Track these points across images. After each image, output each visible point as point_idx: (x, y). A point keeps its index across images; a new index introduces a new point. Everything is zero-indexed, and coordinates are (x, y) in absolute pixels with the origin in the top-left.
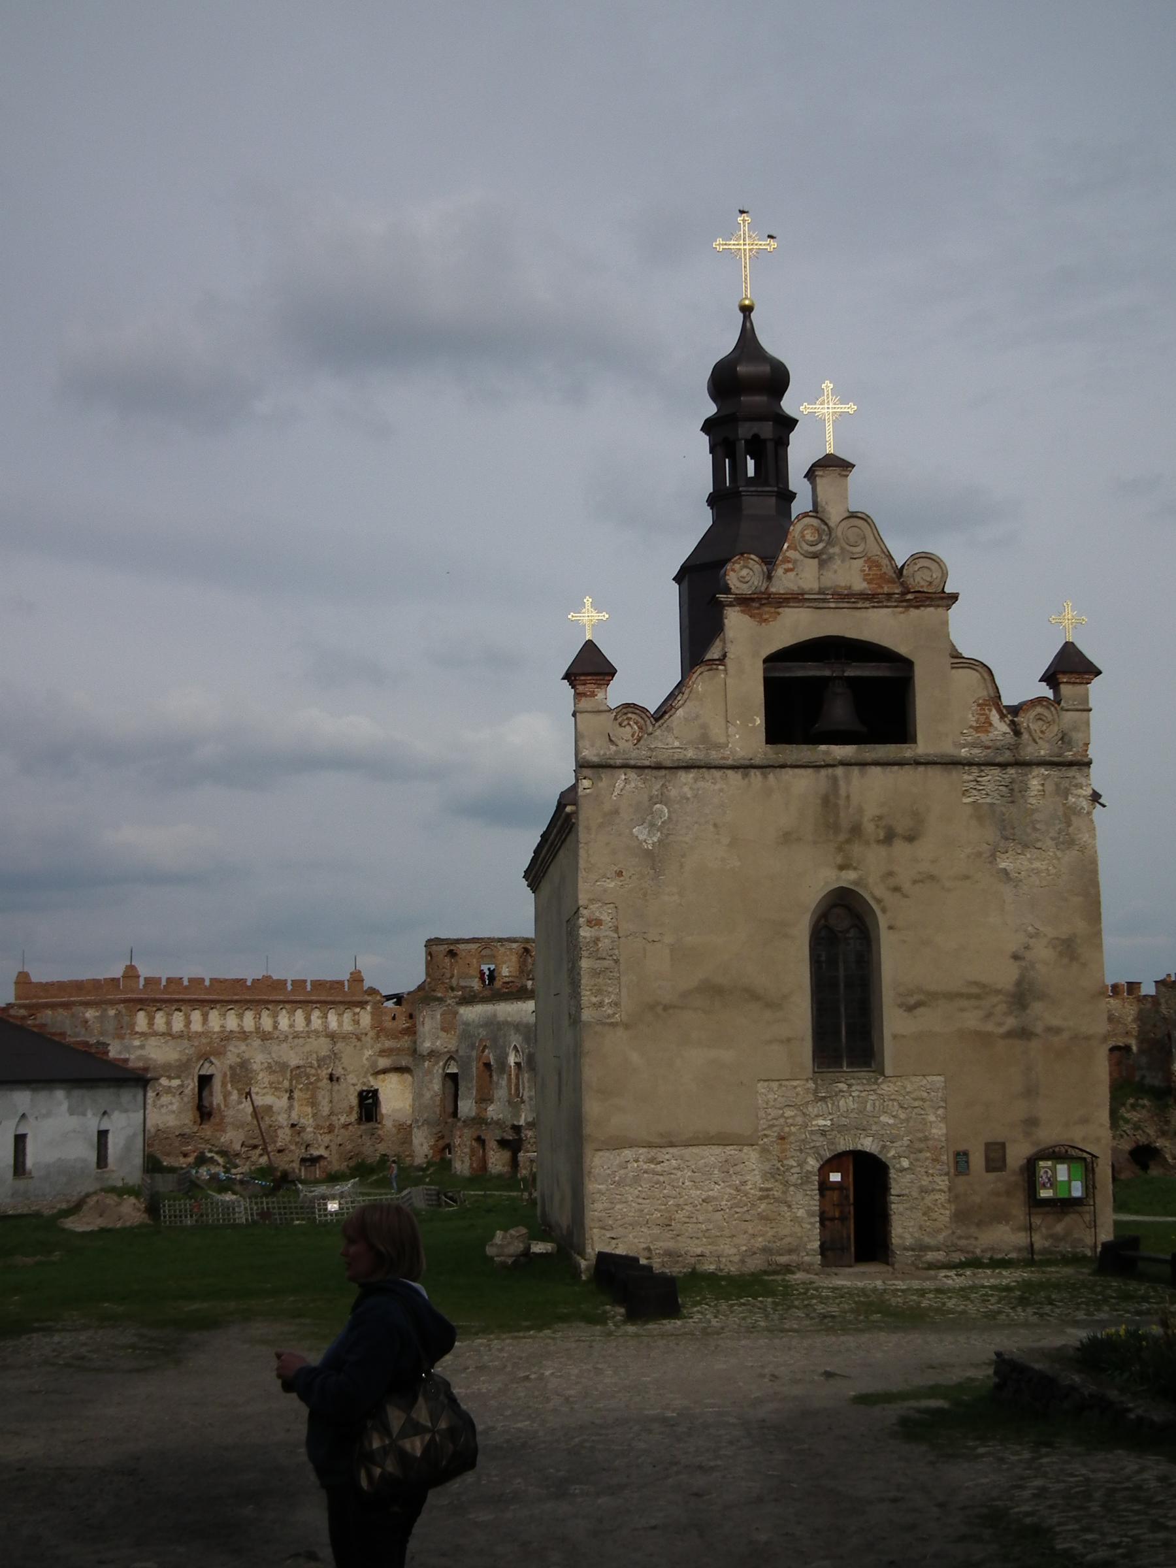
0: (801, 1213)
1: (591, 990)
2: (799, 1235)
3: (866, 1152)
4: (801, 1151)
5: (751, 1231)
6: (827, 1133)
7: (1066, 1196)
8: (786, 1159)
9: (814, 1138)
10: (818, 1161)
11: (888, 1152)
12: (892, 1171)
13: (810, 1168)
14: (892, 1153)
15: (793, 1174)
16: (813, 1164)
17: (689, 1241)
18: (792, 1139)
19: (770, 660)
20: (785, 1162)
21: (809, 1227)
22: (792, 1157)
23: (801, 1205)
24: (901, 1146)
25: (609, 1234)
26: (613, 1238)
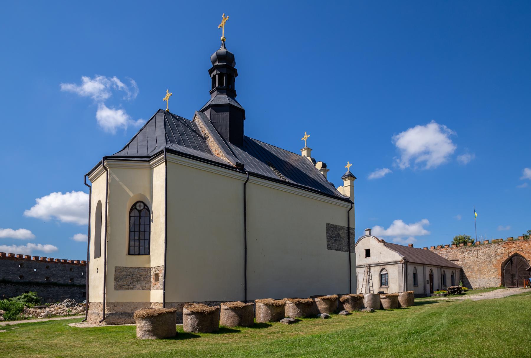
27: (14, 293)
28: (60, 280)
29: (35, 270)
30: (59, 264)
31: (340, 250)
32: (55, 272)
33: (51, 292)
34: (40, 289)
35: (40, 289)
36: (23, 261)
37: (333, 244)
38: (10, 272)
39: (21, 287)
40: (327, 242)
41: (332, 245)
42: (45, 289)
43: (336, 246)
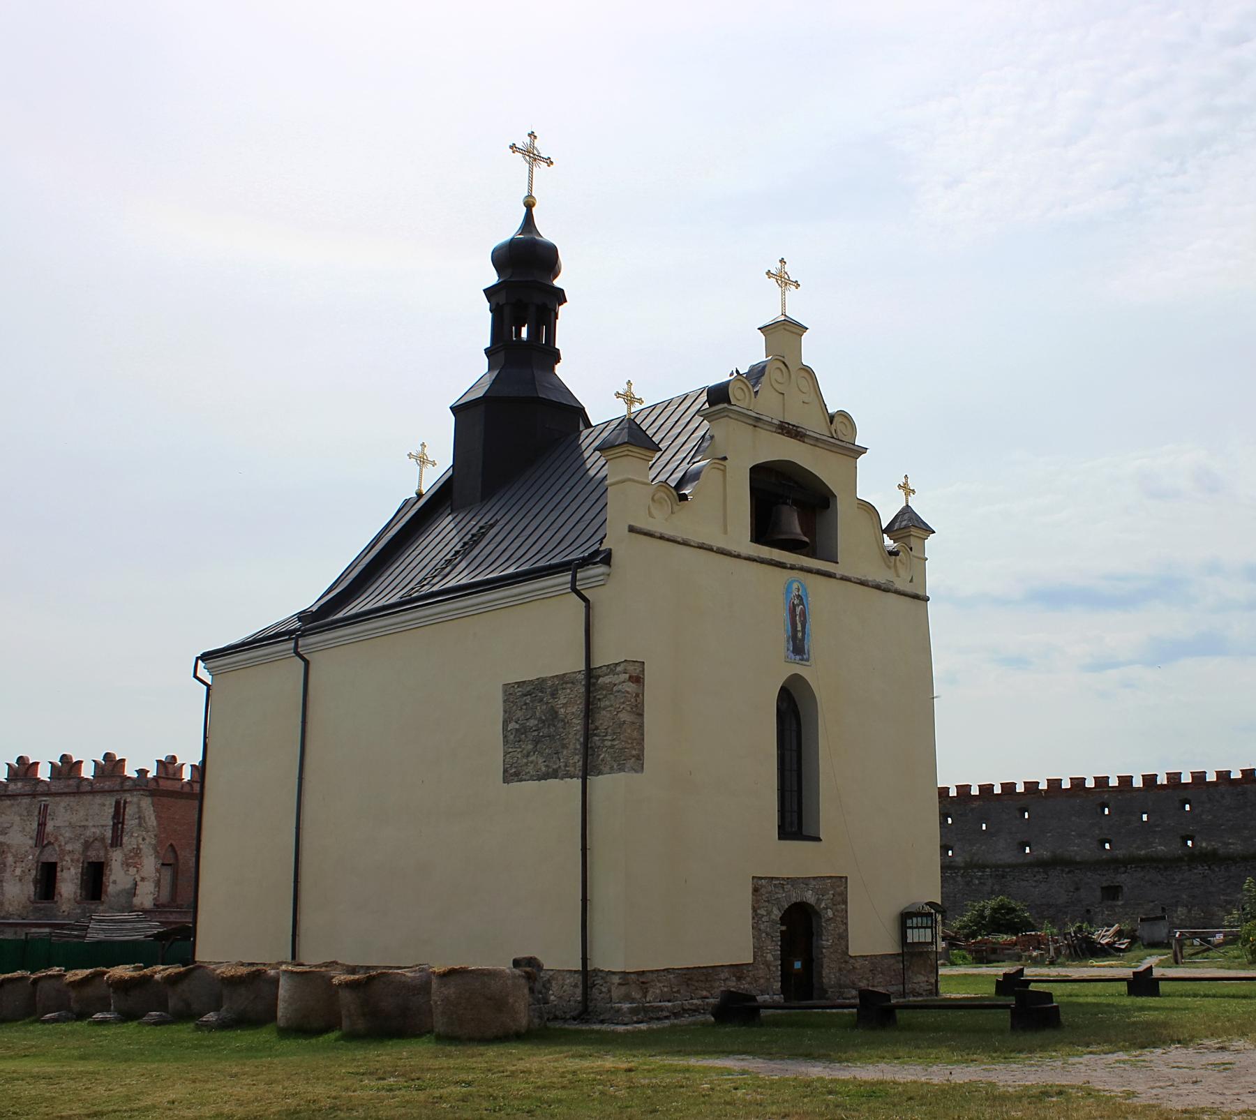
0: (769, 957)
1: (632, 743)
2: (768, 977)
3: (807, 903)
4: (768, 901)
5: (738, 974)
6: (785, 887)
7: (917, 941)
8: (759, 908)
9: (777, 891)
10: (780, 911)
11: (821, 904)
12: (823, 920)
13: (773, 917)
14: (823, 905)
15: (764, 922)
16: (777, 914)
17: (696, 984)
18: (763, 891)
19: (757, 471)
20: (759, 911)
21: (774, 969)
22: (763, 907)
23: (769, 950)
24: (828, 899)
25: (641, 980)
26: (643, 983)
27: (1071, 894)
28: (1230, 841)
29: (1145, 817)
30: (1222, 788)
31: (554, 774)
32: (1210, 817)
33: (1182, 883)
34: (1147, 878)
35: (1147, 878)
36: (1106, 796)
37: (528, 756)
38: (1073, 833)
39: (1089, 874)
40: (505, 754)
41: (525, 761)
42: (1162, 875)
43: (541, 760)
